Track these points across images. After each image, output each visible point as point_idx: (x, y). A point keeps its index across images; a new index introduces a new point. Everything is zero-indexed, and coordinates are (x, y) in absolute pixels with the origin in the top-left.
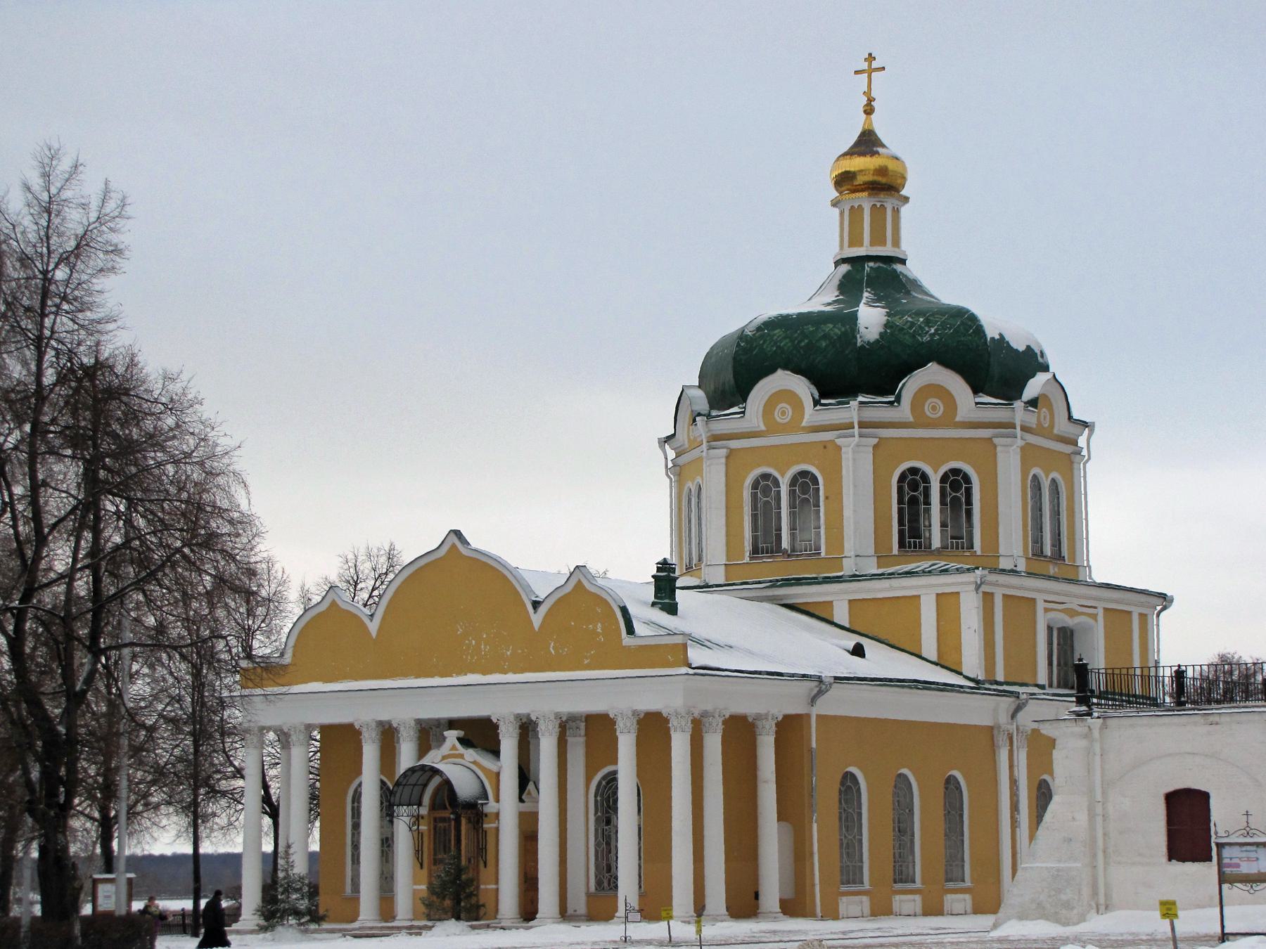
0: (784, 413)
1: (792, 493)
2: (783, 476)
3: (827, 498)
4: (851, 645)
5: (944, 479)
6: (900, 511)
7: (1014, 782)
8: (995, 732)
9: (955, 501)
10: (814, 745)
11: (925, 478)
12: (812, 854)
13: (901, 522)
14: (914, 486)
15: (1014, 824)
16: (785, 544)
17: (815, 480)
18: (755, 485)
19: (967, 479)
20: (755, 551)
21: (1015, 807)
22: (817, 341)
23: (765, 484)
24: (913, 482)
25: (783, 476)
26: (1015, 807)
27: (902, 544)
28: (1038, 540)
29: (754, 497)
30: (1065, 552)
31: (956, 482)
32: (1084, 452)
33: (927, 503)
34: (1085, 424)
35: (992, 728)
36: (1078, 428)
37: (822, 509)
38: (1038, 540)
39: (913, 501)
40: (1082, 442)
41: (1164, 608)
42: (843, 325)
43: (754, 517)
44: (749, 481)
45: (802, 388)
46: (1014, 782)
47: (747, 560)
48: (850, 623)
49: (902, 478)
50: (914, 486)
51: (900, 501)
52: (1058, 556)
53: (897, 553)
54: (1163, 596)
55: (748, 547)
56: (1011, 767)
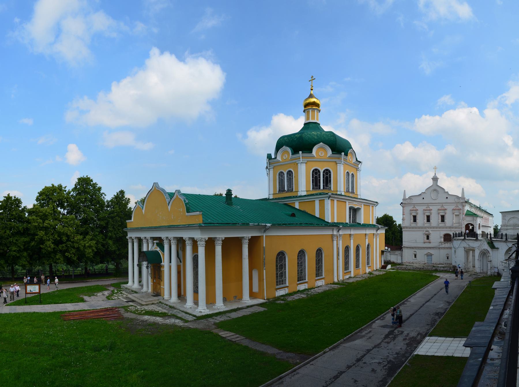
0: (286, 157)
1: (287, 176)
2: (285, 172)
3: (295, 177)
4: (290, 213)
5: (324, 172)
6: (313, 180)
7: (338, 249)
8: (333, 236)
9: (327, 178)
10: (264, 246)
11: (319, 171)
12: (263, 280)
13: (313, 183)
14: (316, 173)
15: (338, 259)
16: (286, 189)
17: (292, 173)
18: (279, 175)
19: (330, 172)
20: (279, 190)
21: (338, 255)
22: (294, 139)
23: (281, 174)
24: (316, 172)
25: (285, 172)
26: (338, 255)
27: (313, 188)
28: (348, 188)
29: (279, 177)
30: (355, 191)
31: (327, 172)
32: (360, 168)
33: (320, 177)
34: (360, 162)
35: (332, 235)
36: (358, 163)
37: (294, 180)
38: (348, 188)
39: (316, 178)
40: (359, 166)
41: (377, 205)
42: (300, 134)
43: (279, 182)
44: (278, 174)
45: (289, 150)
46: (338, 249)
47: (277, 193)
48: (299, 207)
49: (313, 171)
50: (316, 173)
51: (313, 177)
52: (353, 192)
53: (311, 190)
54: (377, 202)
55: (278, 190)
56: (337, 244)
